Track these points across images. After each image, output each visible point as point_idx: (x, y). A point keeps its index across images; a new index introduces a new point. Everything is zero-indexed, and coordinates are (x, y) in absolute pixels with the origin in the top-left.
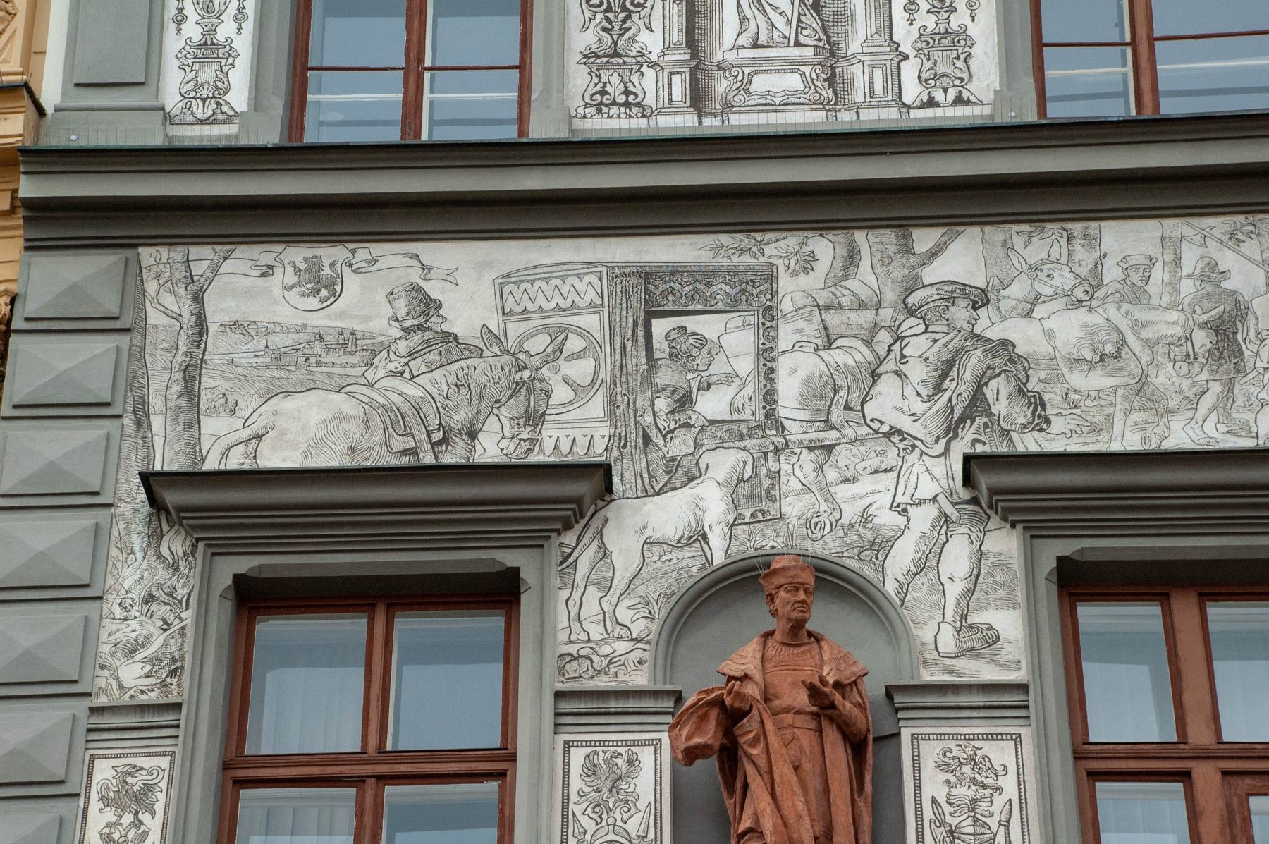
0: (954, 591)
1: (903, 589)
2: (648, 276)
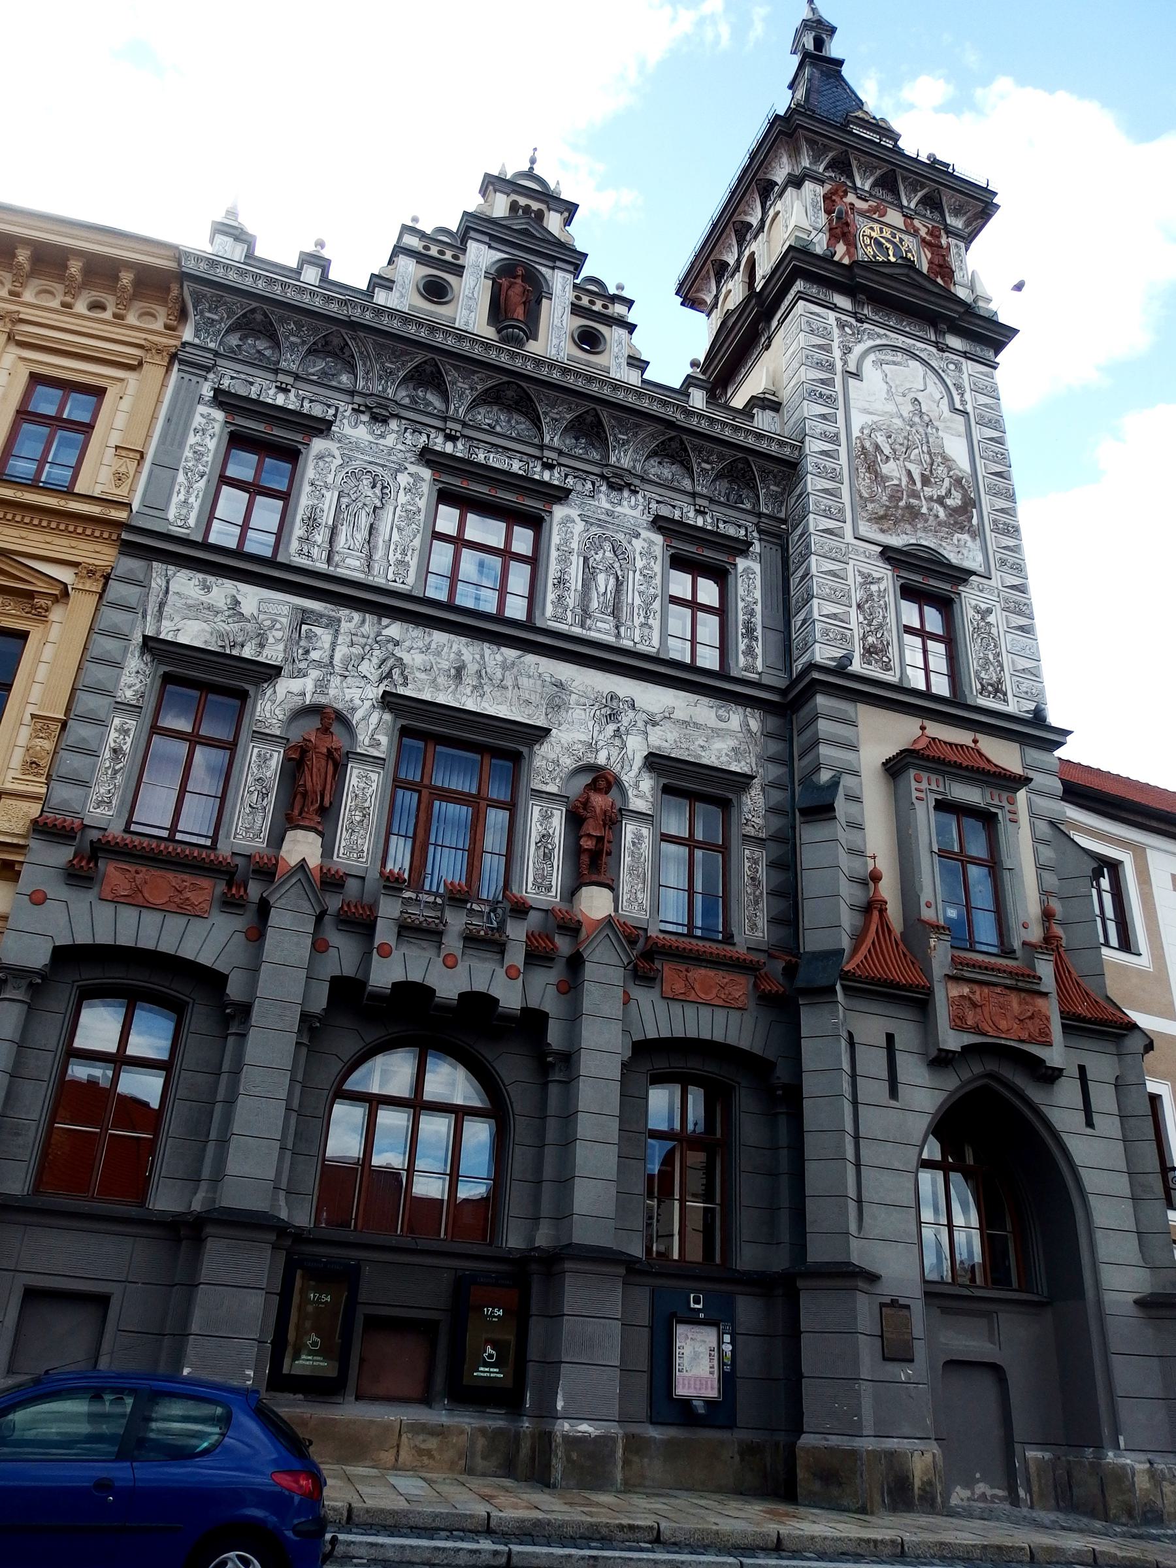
0: (372, 727)
1: (358, 724)
2: (304, 611)
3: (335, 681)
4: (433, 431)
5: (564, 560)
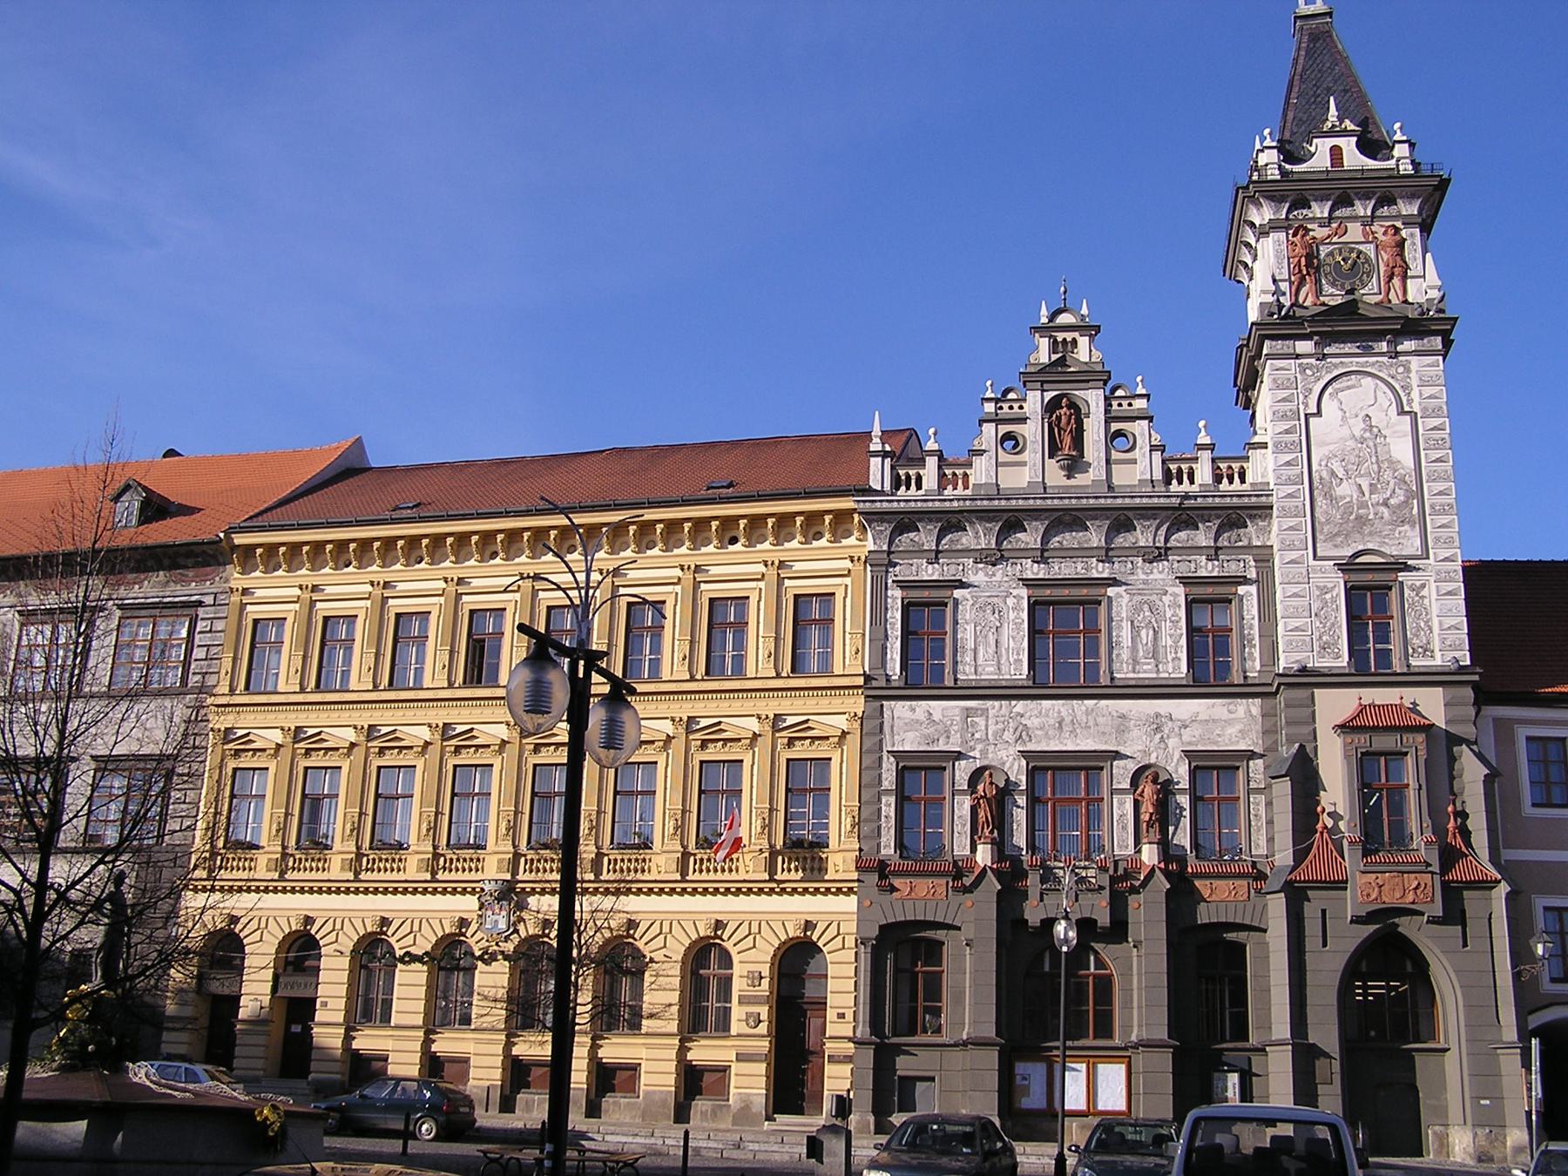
5: (1120, 627)
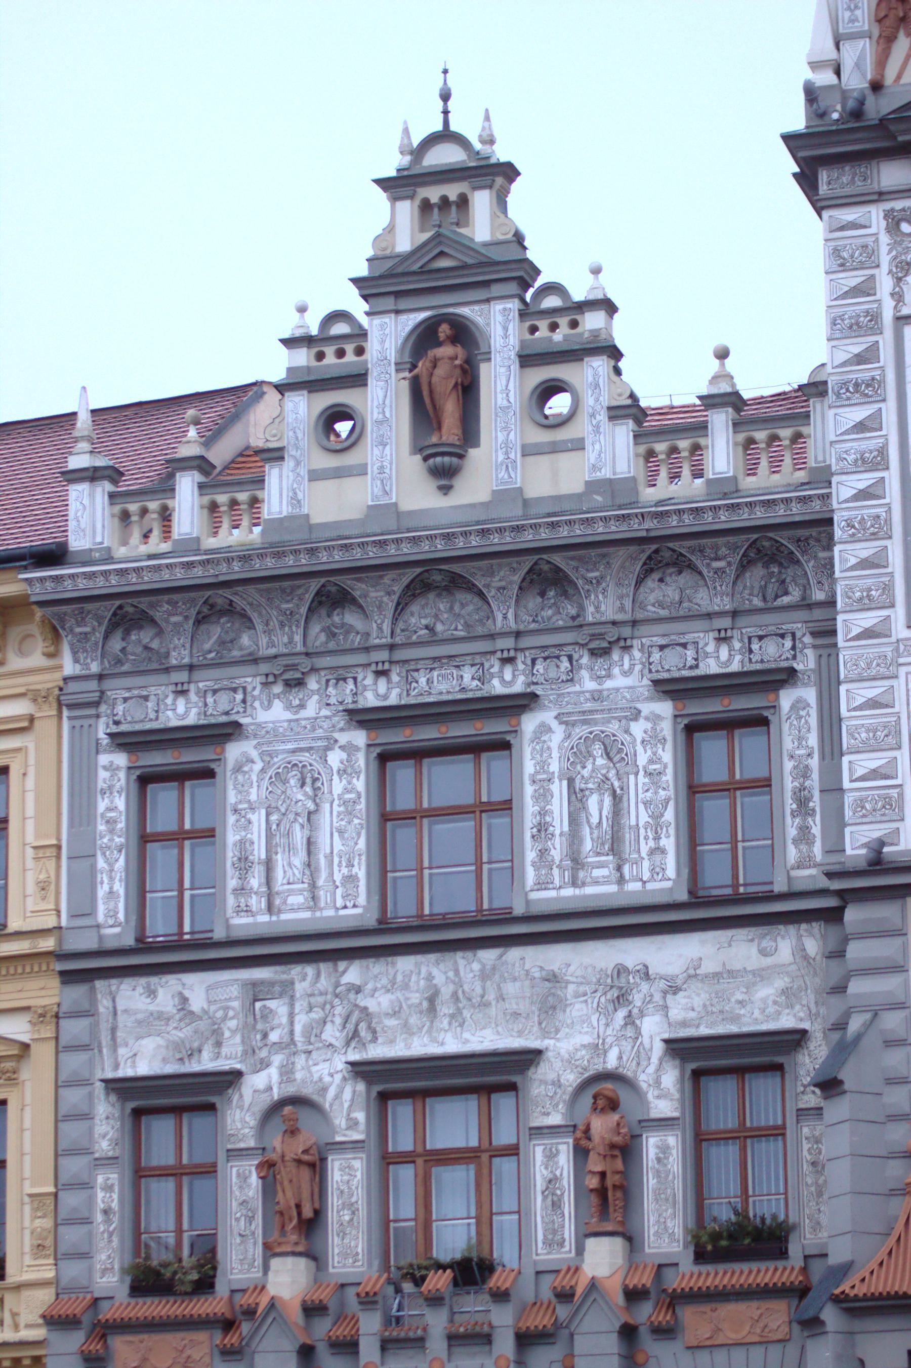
0: (346, 1105)
1: (331, 1105)
2: (254, 984)
3: (300, 1061)
4: (359, 670)
5: (543, 796)
